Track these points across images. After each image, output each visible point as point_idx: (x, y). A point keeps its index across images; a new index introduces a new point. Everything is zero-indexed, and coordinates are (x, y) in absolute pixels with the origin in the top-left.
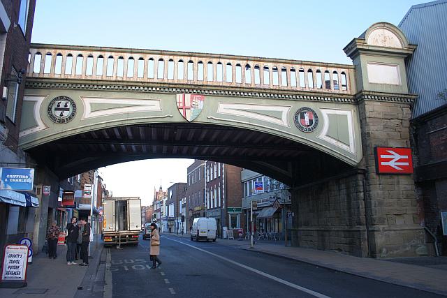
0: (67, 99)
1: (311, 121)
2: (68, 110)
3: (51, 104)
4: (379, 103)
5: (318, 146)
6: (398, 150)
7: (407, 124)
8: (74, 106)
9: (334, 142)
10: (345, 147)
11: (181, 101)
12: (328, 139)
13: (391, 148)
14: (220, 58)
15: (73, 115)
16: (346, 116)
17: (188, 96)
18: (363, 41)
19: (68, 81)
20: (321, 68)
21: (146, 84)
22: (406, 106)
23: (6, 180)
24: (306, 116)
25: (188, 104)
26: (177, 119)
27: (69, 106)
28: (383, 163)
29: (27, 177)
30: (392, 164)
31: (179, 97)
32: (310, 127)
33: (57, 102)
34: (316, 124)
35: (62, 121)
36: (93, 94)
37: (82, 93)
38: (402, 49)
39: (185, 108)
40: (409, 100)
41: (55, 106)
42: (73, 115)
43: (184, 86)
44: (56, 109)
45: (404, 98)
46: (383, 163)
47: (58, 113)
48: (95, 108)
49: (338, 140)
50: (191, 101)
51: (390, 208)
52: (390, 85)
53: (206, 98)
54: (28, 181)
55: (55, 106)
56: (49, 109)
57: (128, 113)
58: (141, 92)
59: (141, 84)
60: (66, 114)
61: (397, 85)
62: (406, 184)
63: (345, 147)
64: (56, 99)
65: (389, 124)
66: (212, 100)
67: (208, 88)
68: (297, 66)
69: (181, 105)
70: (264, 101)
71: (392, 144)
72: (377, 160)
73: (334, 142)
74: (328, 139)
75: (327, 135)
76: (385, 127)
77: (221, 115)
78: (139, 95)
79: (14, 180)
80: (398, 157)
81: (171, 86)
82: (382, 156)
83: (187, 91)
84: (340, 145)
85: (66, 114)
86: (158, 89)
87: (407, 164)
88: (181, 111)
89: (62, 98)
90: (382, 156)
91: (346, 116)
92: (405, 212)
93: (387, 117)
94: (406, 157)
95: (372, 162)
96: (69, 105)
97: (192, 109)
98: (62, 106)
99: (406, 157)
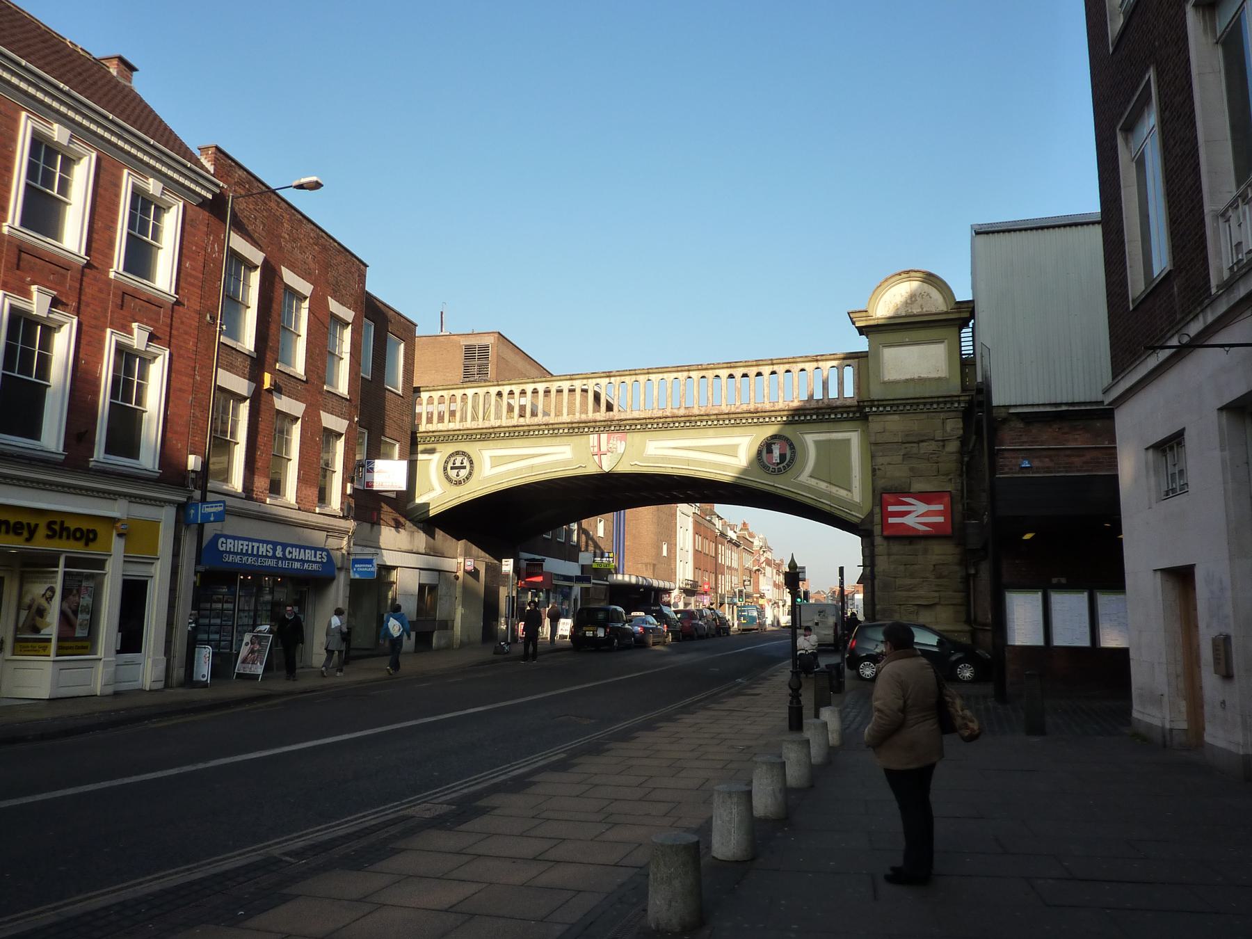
0: (464, 454)
1: (783, 457)
2: (464, 468)
3: (446, 462)
4: (896, 417)
5: (793, 496)
6: (925, 497)
7: (953, 446)
8: (471, 462)
9: (823, 486)
10: (843, 493)
11: (596, 444)
12: (813, 482)
13: (909, 494)
14: (649, 373)
15: (470, 474)
16: (848, 441)
17: (604, 437)
18: (864, 314)
19: (462, 432)
20: (807, 366)
21: (551, 427)
22: (952, 414)
23: (355, 569)
24: (776, 452)
25: (604, 448)
26: (592, 469)
27: (466, 463)
28: (891, 520)
29: (371, 566)
30: (909, 521)
31: (593, 438)
32: (781, 466)
33: (452, 459)
34: (792, 459)
35: (459, 483)
36: (491, 444)
37: (478, 445)
38: (946, 313)
39: (600, 454)
40: (956, 405)
41: (450, 465)
42: (470, 474)
43: (598, 424)
44: (452, 468)
45: (945, 403)
46: (891, 520)
47: (453, 473)
48: (496, 461)
49: (830, 483)
50: (608, 443)
51: (905, 594)
52: (921, 380)
53: (629, 436)
54: (372, 569)
55: (450, 465)
56: (445, 469)
57: (532, 467)
58: (544, 436)
59: (544, 427)
60: (463, 473)
61: (939, 379)
62: (942, 553)
63: (843, 493)
64: (451, 455)
65: (915, 450)
66: (635, 438)
67: (628, 422)
68: (767, 367)
69: (596, 449)
70: (711, 432)
71: (918, 486)
72: (885, 515)
73: (823, 486)
74: (813, 482)
75: (811, 476)
76: (906, 457)
77: (648, 459)
78: (545, 441)
79: (361, 569)
80: (921, 507)
81: (581, 425)
82: (891, 508)
83: (602, 429)
84: (834, 490)
85: (463, 473)
86: (566, 431)
87: (941, 519)
88: (596, 457)
89: (457, 453)
90: (891, 508)
91: (848, 441)
92: (936, 600)
93: (910, 439)
94: (941, 507)
95: (877, 518)
96: (465, 461)
97: (609, 454)
98: (458, 464)
99: (941, 507)
